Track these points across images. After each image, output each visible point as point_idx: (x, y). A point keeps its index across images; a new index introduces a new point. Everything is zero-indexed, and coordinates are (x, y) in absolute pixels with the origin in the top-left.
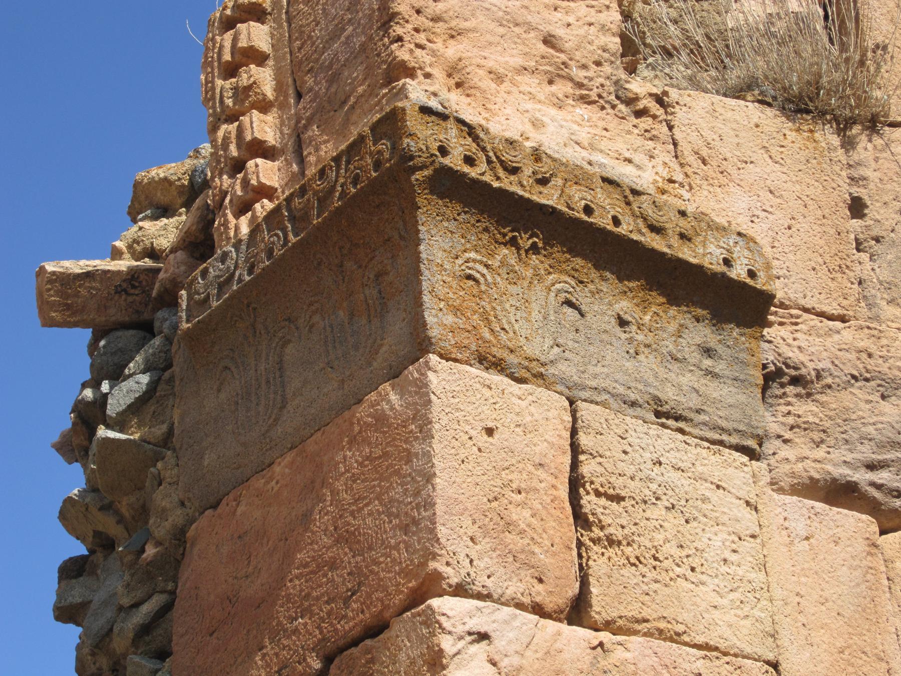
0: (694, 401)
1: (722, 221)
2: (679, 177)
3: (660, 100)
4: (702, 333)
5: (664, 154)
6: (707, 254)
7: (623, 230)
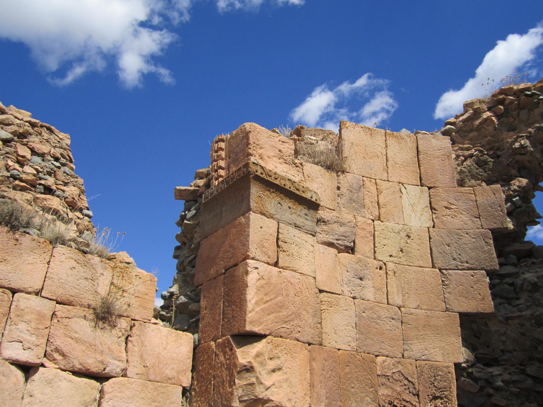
0: (303, 224)
1: (311, 189)
2: (303, 180)
3: (301, 164)
4: (305, 211)
5: (301, 175)
6: (308, 195)
7: (291, 189)
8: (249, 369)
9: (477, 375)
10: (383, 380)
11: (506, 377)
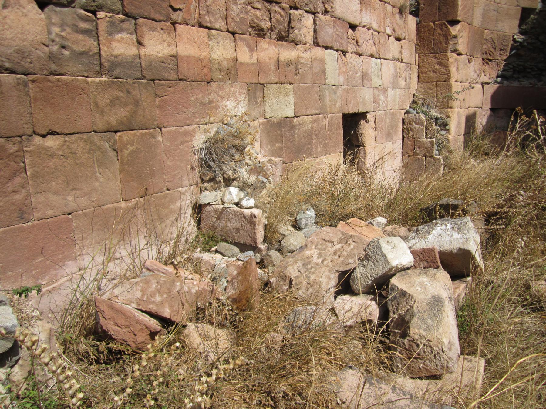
8: (455, 37)
9: (517, 39)
10: (485, 41)
11: (529, 41)
